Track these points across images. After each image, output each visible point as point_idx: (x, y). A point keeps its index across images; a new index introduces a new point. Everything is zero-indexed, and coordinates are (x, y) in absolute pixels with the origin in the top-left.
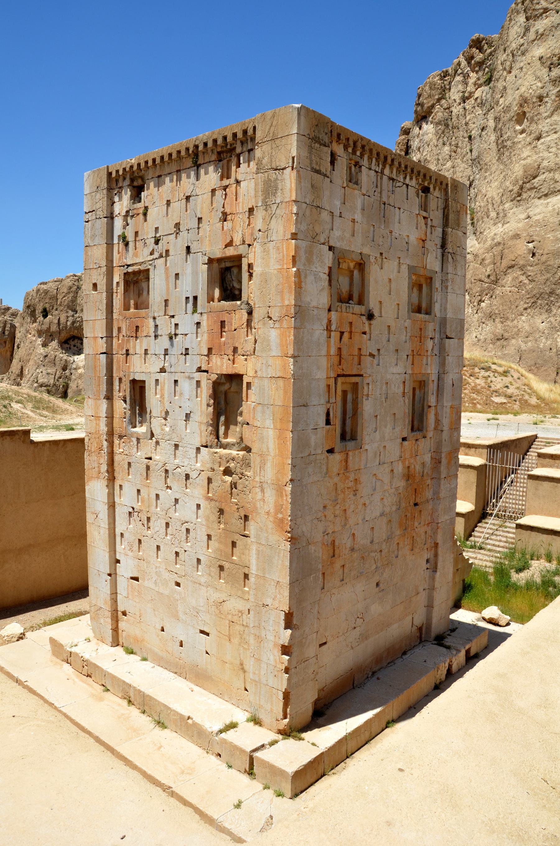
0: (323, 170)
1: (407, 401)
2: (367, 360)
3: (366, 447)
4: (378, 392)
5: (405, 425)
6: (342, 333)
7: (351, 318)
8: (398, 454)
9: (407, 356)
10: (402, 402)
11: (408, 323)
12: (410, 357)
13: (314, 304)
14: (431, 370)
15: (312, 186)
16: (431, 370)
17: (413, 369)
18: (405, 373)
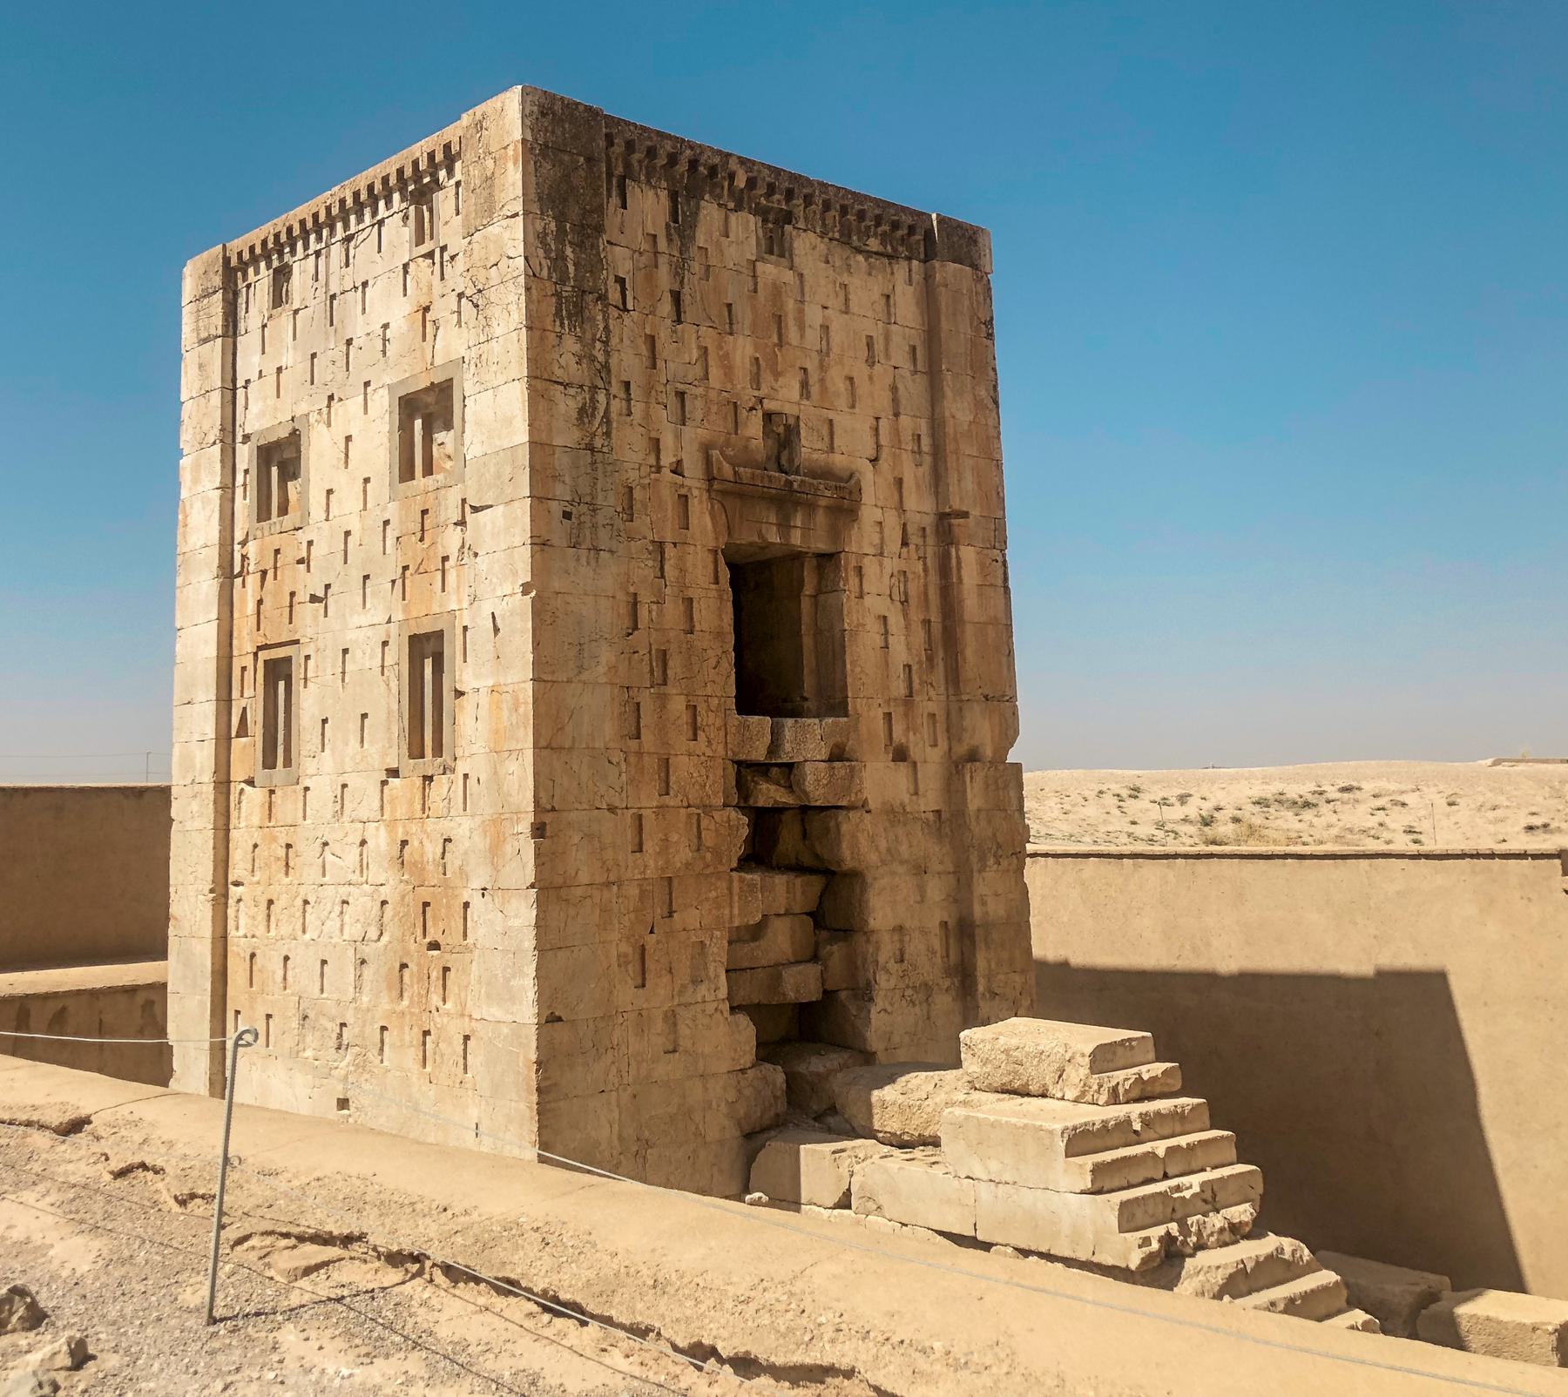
0: (213, 332)
1: (394, 684)
2: (306, 612)
3: (307, 783)
4: (329, 672)
5: (390, 739)
6: (264, 573)
7: (277, 541)
8: (377, 804)
9: (393, 582)
10: (383, 686)
11: (392, 511)
12: (399, 583)
13: (200, 543)
14: (460, 601)
15: (201, 366)
16: (460, 601)
17: (406, 610)
18: (389, 621)
